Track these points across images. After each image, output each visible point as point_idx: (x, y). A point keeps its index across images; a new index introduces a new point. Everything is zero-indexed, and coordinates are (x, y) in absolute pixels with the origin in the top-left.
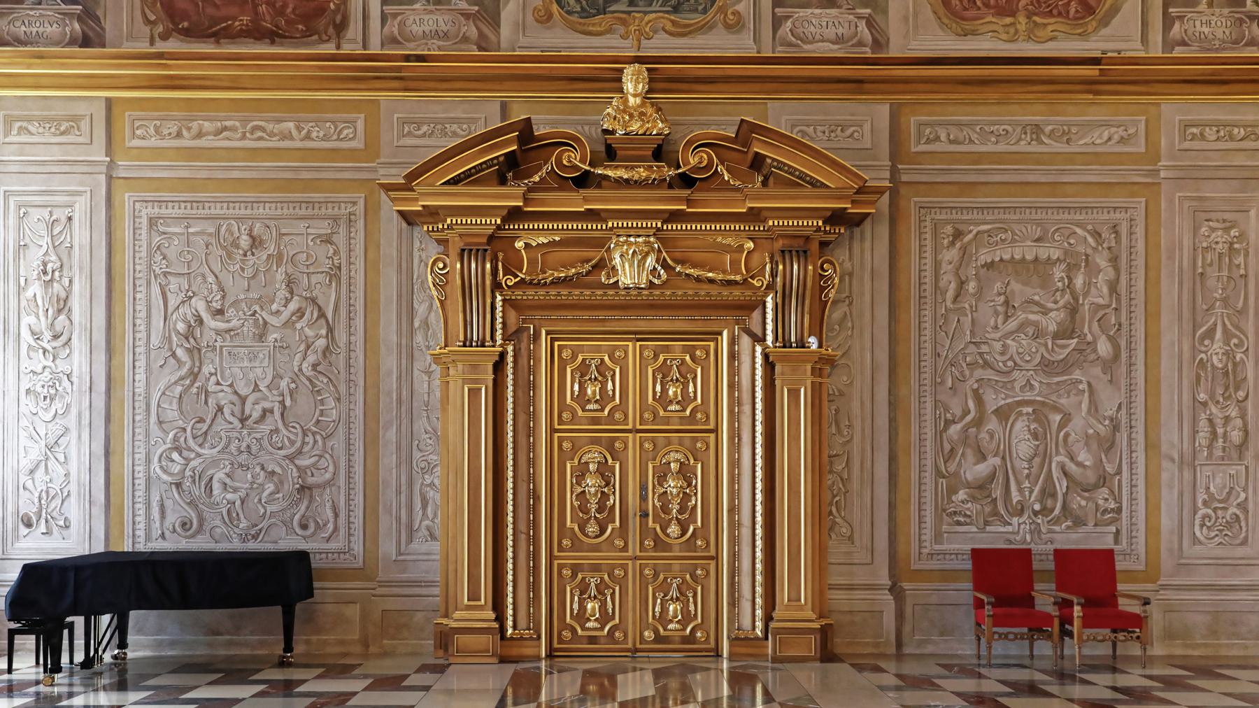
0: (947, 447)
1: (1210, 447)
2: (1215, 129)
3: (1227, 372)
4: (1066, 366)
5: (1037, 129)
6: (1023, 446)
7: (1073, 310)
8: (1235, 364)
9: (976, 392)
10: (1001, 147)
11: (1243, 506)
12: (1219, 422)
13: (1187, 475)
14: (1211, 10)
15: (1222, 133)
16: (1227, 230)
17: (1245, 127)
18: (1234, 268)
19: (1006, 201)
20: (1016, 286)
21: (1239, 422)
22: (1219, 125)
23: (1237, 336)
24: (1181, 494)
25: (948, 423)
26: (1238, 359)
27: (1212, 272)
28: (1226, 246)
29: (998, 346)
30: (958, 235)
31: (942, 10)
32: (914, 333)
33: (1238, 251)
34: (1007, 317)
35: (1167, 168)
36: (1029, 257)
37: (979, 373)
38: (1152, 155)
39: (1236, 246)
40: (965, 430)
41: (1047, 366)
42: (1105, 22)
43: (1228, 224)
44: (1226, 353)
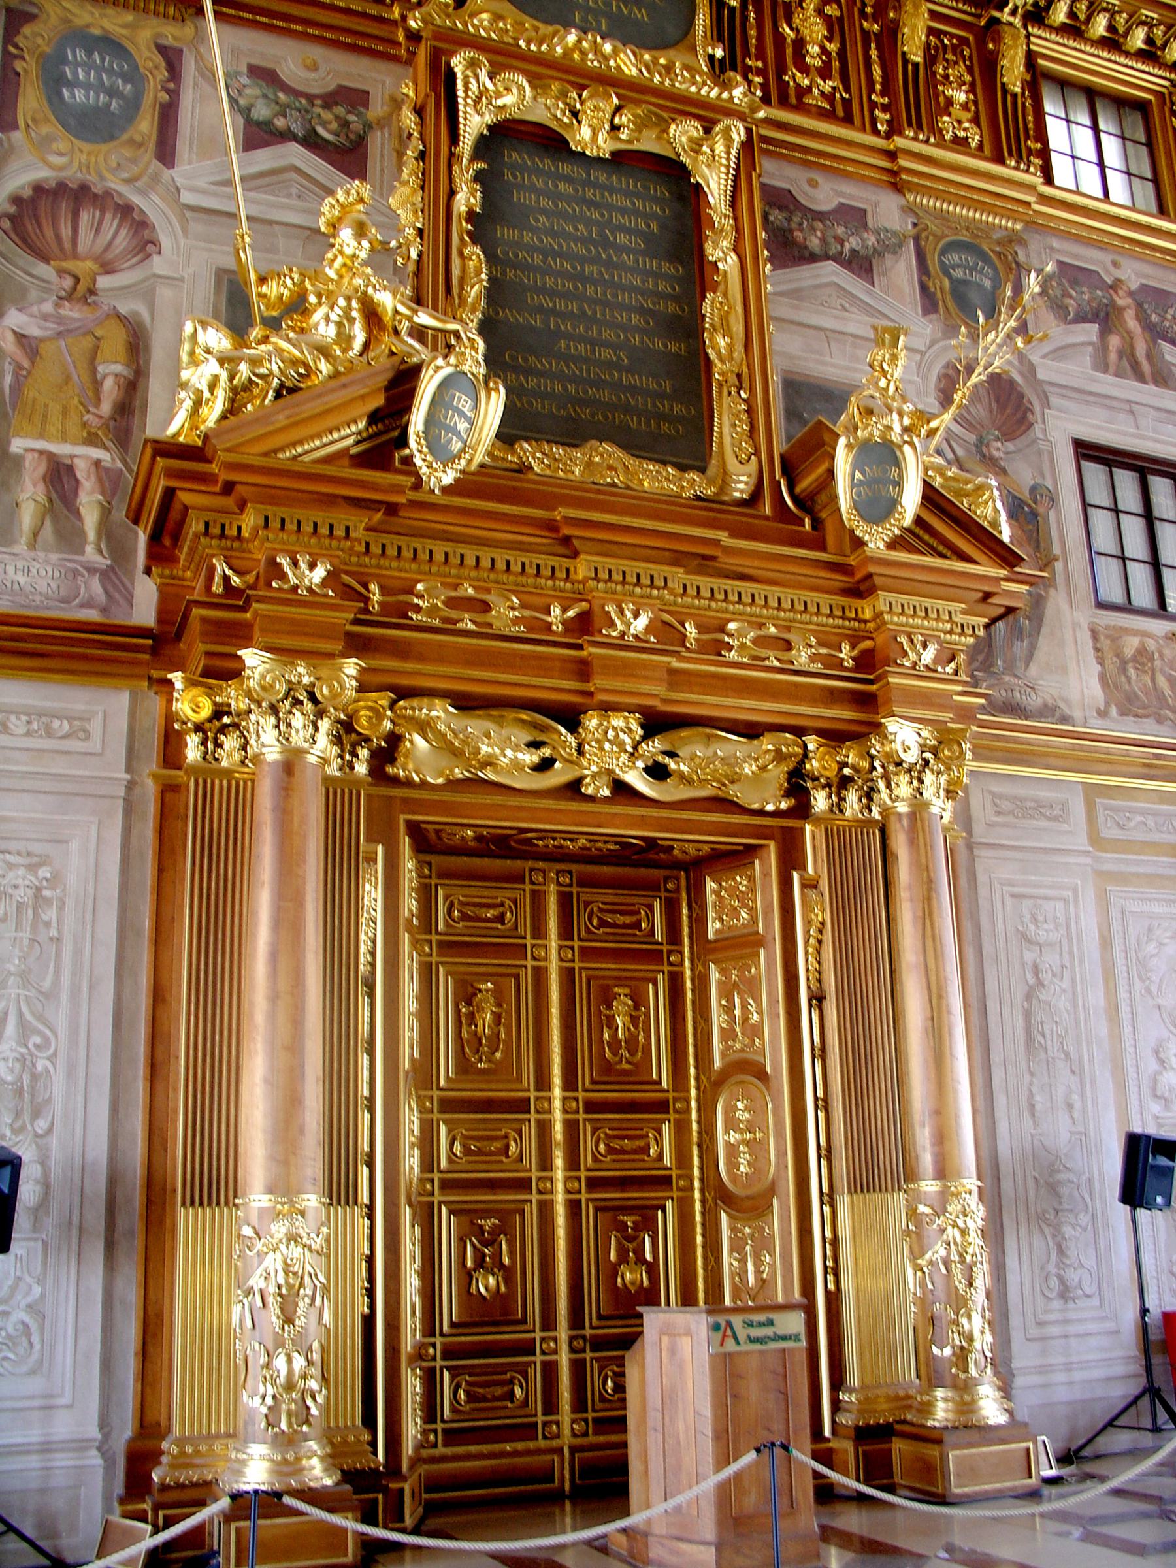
2: (24, 718)
3: (22, 1088)
8: (34, 1077)
14: (33, 554)
15: (35, 726)
16: (32, 868)
17: (70, 719)
18: (41, 926)
22: (30, 713)
23: (39, 1033)
26: (39, 1068)
28: (30, 892)
33: (48, 901)
39: (46, 893)
43: (35, 860)
44: (22, 1059)
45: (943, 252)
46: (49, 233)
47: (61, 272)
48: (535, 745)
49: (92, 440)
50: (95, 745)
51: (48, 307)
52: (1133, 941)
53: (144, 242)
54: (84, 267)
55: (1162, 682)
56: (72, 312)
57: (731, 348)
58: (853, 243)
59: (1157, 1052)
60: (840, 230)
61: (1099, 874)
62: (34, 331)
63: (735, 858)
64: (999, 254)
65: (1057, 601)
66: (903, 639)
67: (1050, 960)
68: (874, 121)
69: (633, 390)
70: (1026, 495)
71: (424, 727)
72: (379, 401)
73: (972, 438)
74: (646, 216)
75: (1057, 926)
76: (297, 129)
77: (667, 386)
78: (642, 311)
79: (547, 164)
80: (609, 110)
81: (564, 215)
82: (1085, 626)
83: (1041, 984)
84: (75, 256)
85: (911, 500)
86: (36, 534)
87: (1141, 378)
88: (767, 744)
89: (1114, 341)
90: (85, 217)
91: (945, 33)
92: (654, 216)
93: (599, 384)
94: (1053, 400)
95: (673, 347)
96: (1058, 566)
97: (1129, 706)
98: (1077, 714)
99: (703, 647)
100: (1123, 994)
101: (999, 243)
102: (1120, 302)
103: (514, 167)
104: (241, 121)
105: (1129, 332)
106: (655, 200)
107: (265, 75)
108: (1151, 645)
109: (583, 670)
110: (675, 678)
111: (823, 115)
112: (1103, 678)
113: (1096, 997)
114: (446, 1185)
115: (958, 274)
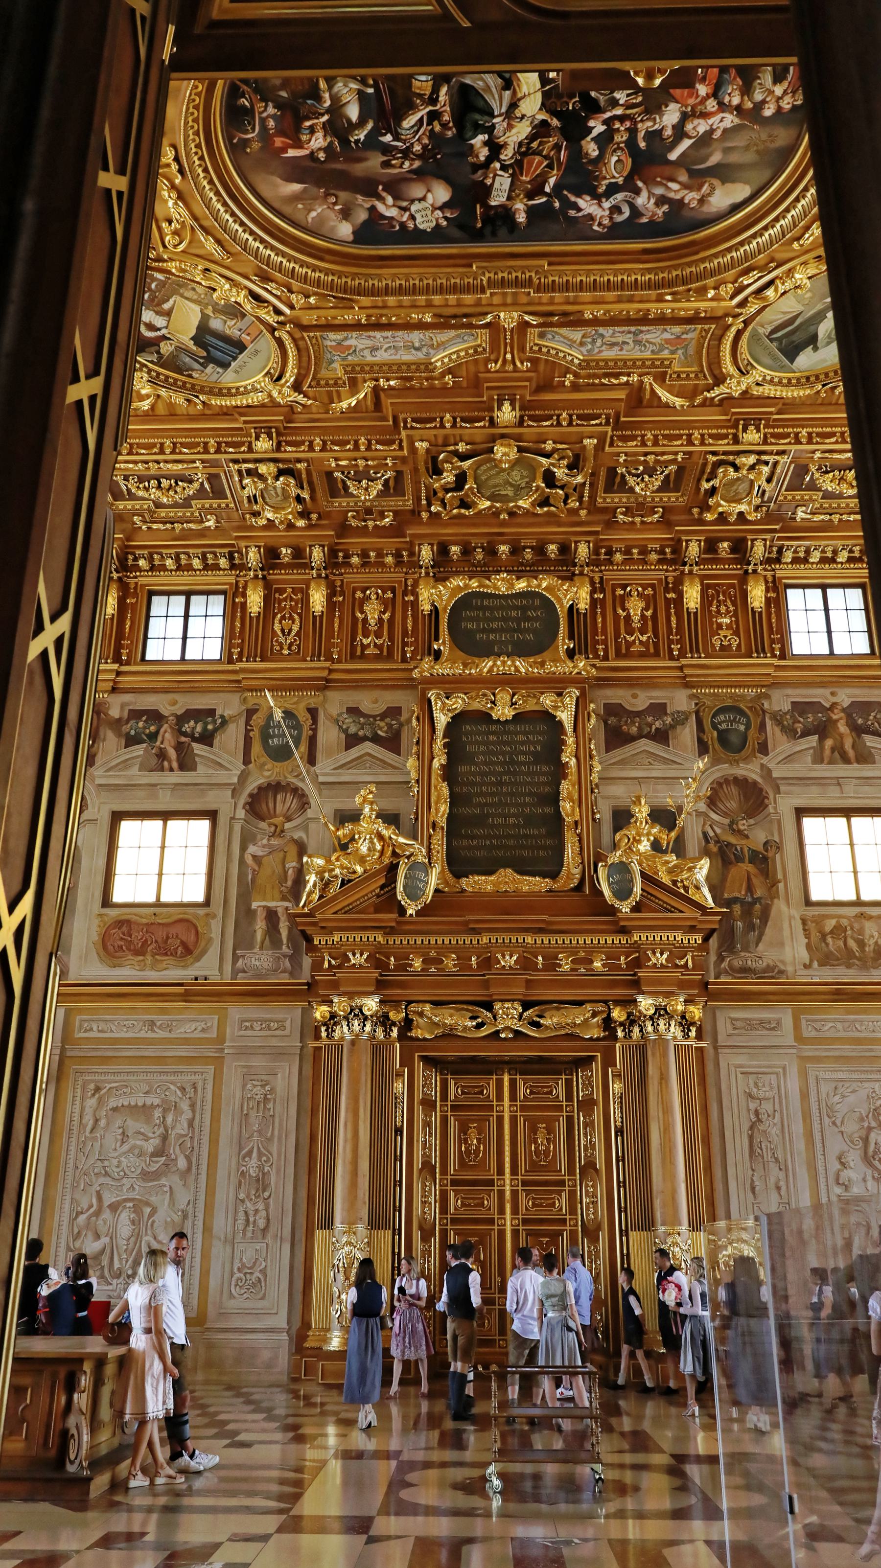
0: (76, 1230)
1: (244, 1231)
4: (155, 1176)
5: (152, 1023)
6: (125, 1229)
7: (165, 1138)
9: (98, 1193)
10: (130, 1035)
11: (263, 1272)
12: (251, 1213)
13: (229, 1249)
16: (263, 1086)
19: (128, 1068)
20: (130, 1122)
21: (264, 1213)
22: (262, 1021)
24: (224, 1264)
25: (78, 1214)
27: (253, 1114)
29: (115, 1162)
30: (97, 1089)
31: (102, 953)
32: (63, 1154)
34: (123, 1142)
35: (229, 1047)
36: (140, 1104)
37: (102, 1180)
38: (221, 1039)
40: (89, 1218)
41: (146, 1176)
42: (198, 959)
45: (714, 716)
46: (264, 807)
47: (270, 825)
48: (473, 1018)
49: (284, 899)
50: (287, 1032)
51: (265, 841)
52: (824, 1096)
53: (304, 803)
54: (278, 820)
55: (852, 943)
56: (275, 842)
57: (573, 808)
58: (658, 724)
59: (839, 1158)
60: (650, 719)
61: (801, 1058)
62: (260, 853)
63: (585, 1062)
64: (750, 708)
65: (779, 907)
66: (649, 953)
67: (767, 1107)
68: (671, 651)
69: (526, 836)
70: (761, 848)
71: (421, 1014)
72: (383, 881)
73: (727, 821)
74: (534, 743)
75: (771, 1088)
76: (369, 734)
77: (543, 831)
78: (530, 794)
79: (483, 728)
80: (508, 698)
81: (492, 753)
82: (798, 917)
83: (759, 1120)
84: (275, 816)
85: (637, 889)
86: (262, 943)
87: (846, 760)
88: (589, 1007)
89: (829, 743)
90: (279, 797)
91: (718, 585)
92: (538, 741)
93: (509, 837)
94: (782, 788)
95: (547, 810)
96: (781, 885)
97: (827, 960)
98: (790, 969)
99: (546, 968)
100: (816, 1126)
101: (751, 701)
102: (835, 717)
103: (467, 734)
104: (343, 736)
105: (841, 736)
106: (540, 733)
107: (354, 711)
108: (845, 922)
109: (486, 985)
110: (529, 984)
111: (642, 655)
112: (808, 947)
113: (798, 1128)
114: (454, 1221)
115: (724, 726)
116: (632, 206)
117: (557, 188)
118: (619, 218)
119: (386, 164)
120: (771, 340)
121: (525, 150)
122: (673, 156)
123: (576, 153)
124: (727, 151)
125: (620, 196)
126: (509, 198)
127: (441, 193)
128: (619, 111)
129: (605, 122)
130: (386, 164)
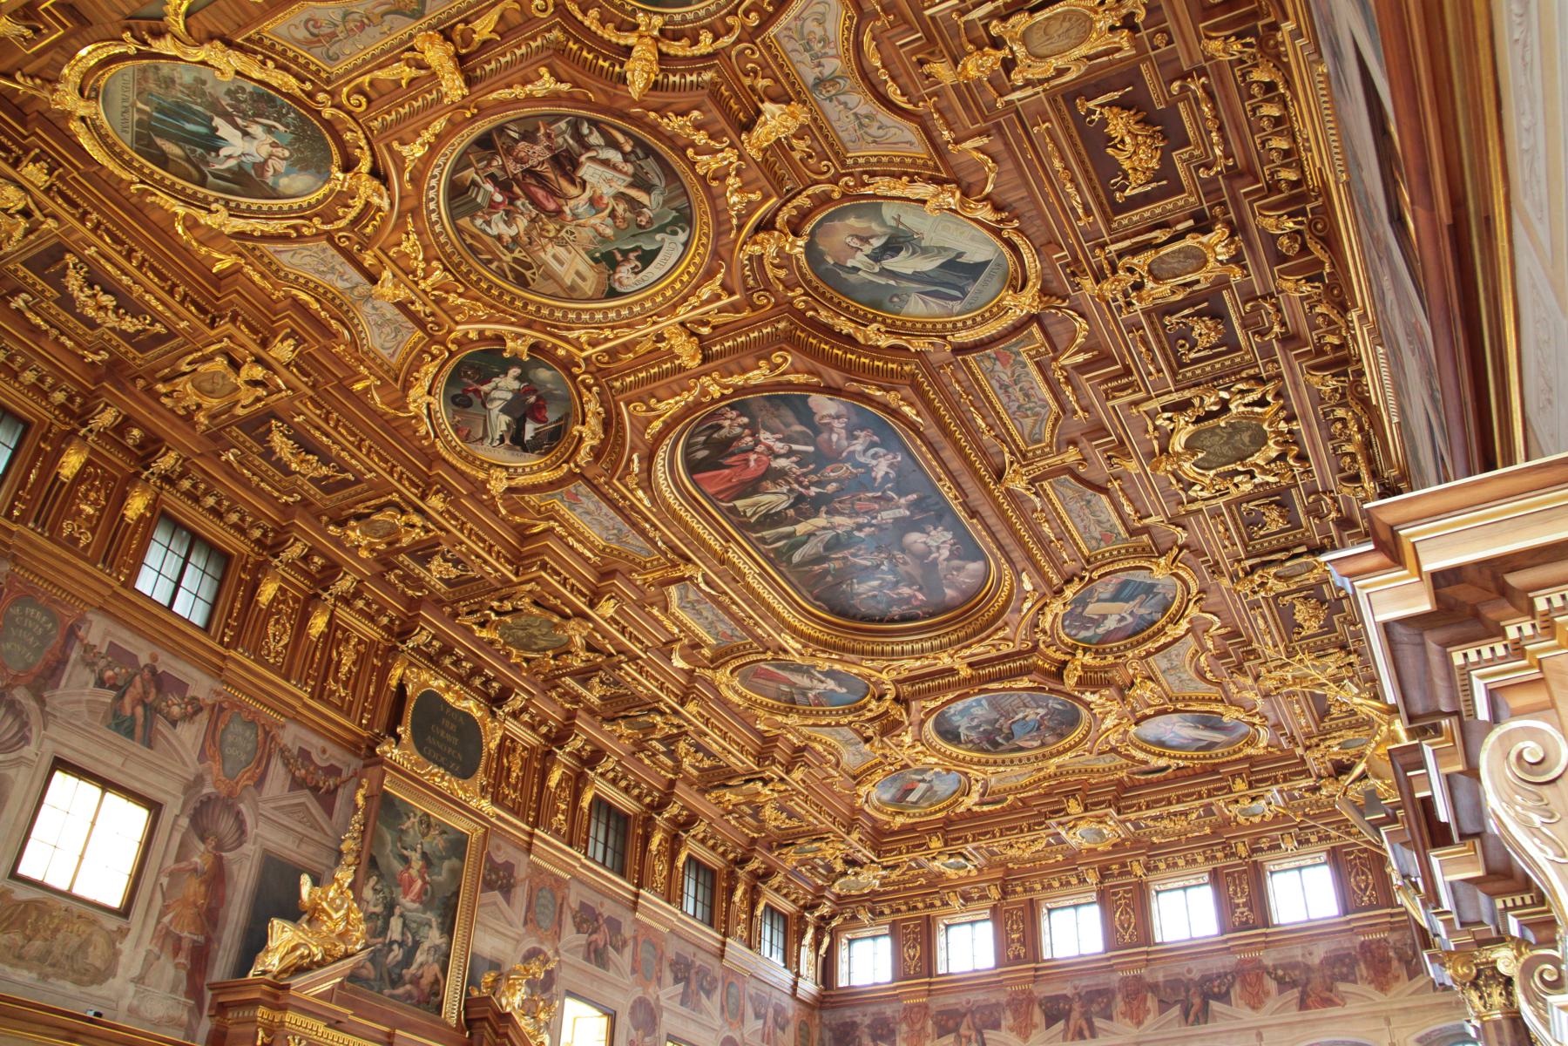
116: (865, 451)
117: (874, 490)
118: (881, 451)
119: (905, 563)
120: (965, 294)
121: (854, 513)
122: (811, 449)
123: (839, 491)
124: (787, 425)
125: (862, 459)
126: (899, 507)
127: (915, 539)
128: (796, 486)
129: (807, 488)
130: (905, 563)
